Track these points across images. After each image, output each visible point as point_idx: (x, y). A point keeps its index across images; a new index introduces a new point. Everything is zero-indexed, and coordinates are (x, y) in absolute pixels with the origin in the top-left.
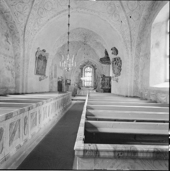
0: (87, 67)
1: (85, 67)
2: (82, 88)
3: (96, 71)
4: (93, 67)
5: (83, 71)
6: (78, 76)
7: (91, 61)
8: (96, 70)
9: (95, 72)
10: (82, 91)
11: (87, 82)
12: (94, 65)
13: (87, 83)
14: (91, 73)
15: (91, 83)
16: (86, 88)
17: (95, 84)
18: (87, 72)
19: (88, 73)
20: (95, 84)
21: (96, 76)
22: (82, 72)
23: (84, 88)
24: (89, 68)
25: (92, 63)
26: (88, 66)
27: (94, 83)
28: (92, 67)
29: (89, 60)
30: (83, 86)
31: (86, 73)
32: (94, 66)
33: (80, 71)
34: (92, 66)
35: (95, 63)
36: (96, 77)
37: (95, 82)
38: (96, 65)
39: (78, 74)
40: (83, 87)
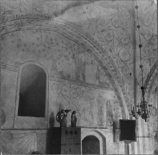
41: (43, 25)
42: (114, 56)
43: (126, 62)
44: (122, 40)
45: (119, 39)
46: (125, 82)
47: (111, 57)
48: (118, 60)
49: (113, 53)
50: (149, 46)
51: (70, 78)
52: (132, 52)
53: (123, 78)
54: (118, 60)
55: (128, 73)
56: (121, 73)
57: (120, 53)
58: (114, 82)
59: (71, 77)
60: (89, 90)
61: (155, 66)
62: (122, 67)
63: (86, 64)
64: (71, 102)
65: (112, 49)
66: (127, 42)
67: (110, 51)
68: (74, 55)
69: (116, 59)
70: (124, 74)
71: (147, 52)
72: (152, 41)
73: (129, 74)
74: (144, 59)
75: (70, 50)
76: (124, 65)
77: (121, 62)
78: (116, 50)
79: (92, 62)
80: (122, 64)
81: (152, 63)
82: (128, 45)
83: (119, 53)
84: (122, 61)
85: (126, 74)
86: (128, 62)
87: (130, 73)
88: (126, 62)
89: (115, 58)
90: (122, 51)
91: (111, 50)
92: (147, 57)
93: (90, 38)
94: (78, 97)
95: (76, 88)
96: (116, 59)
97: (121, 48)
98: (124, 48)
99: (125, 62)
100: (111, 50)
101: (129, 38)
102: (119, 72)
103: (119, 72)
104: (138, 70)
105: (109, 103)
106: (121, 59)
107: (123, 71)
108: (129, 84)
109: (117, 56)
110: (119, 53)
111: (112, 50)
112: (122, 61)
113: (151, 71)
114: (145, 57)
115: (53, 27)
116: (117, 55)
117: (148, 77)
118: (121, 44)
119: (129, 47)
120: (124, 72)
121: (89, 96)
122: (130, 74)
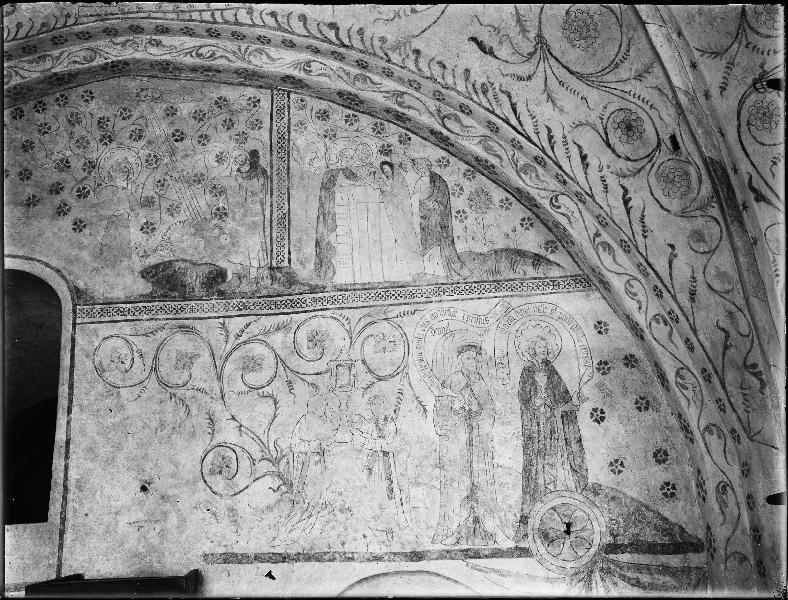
41: (17, 73)
47: (498, 81)
48: (553, 84)
49: (503, 52)
51: (222, 287)
54: (553, 84)
58: (453, 241)
59: (230, 277)
60: (362, 324)
63: (341, 179)
64: (222, 415)
68: (254, 154)
69: (538, 80)
70: (628, 159)
75: (225, 135)
76: (607, 97)
79: (388, 159)
80: (593, 95)
83: (539, 36)
85: (642, 152)
89: (529, 78)
91: (480, 45)
93: (319, 36)
94: (279, 385)
95: (267, 333)
96: (538, 80)
100: (480, 45)
102: (584, 158)
104: (715, 92)
105: (541, 379)
106: (571, 72)
110: (539, 36)
115: (77, 59)
116: (531, 55)
121: (364, 362)
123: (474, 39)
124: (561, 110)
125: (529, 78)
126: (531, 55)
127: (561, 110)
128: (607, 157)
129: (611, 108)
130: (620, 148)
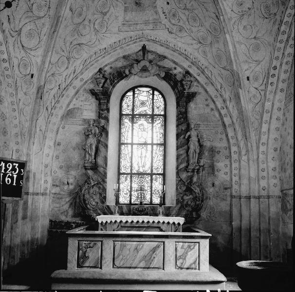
0: (133, 89)
1: (122, 85)
2: (101, 219)
3: (195, 110)
4: (174, 88)
5: (113, 114)
6: (77, 139)
7: (160, 50)
8: (192, 105)
9: (183, 118)
10: (109, 244)
11: (135, 179)
12: (178, 72)
13: (135, 186)
14: (159, 123)
15: (158, 185)
16: (130, 218)
17: (189, 190)
18: (133, 117)
19: (142, 121)
20: (189, 190)
21: (194, 139)
22: (107, 119)
23: (118, 218)
24: (143, 95)
25: (167, 64)
26: (144, 81)
27: (180, 181)
28: (164, 86)
29: (150, 47)
30: (111, 201)
31: (127, 121)
32: (179, 78)
33: (89, 110)
34: (168, 77)
35: (186, 64)
36: (193, 145)
37: (184, 176)
38: (193, 71)
39: (80, 128)
40: (108, 211)
42: (12, 32)
43: (28, 51)
44: (34, 6)
45: (28, 3)
46: (20, 88)
47: (7, 32)
49: (12, 26)
50: (74, 35)
52: (45, 35)
53: (18, 81)
55: (28, 73)
56: (16, 68)
57: (23, 29)
61: (74, 73)
62: (20, 58)
65: (11, 17)
66: (42, 14)
67: (8, 18)
69: (14, 39)
71: (68, 44)
72: (81, 27)
73: (29, 74)
74: (61, 55)
76: (24, 55)
77: (21, 47)
78: (17, 22)
80: (22, 52)
81: (70, 65)
82: (43, 21)
83: (21, 29)
84: (23, 46)
85: (24, 74)
86: (32, 53)
87: (31, 73)
88: (28, 51)
89: (13, 37)
90: (29, 28)
92: (66, 52)
96: (14, 39)
97: (27, 21)
98: (32, 23)
99: (27, 50)
101: (48, 7)
102: (13, 66)
103: (13, 66)
107: (20, 66)
108: (25, 94)
109: (16, 33)
111: (12, 20)
112: (23, 46)
113: (65, 79)
114: (63, 51)
116: (17, 31)
117: (59, 88)
118: (30, 14)
119: (43, 24)
120: (22, 70)
122: (30, 76)
123: (9, 16)
124: (14, 51)
125: (13, 37)
126: (17, 31)
127: (14, 51)
128: (17, 72)
129: (23, 59)
130: (20, 69)
